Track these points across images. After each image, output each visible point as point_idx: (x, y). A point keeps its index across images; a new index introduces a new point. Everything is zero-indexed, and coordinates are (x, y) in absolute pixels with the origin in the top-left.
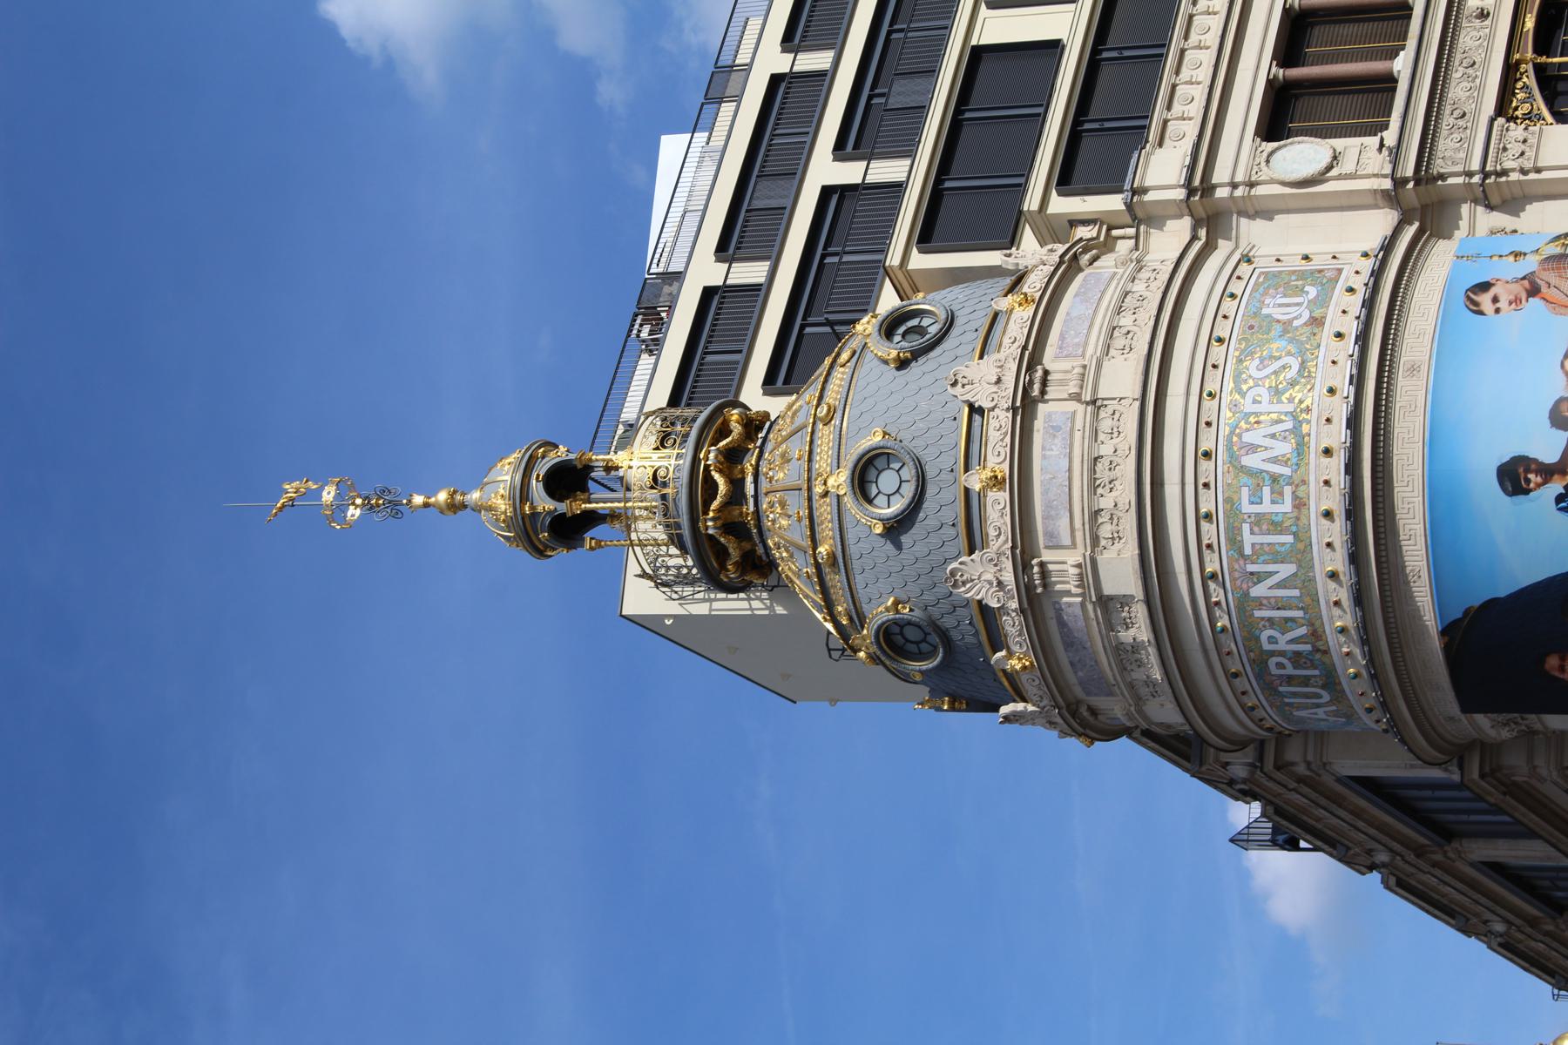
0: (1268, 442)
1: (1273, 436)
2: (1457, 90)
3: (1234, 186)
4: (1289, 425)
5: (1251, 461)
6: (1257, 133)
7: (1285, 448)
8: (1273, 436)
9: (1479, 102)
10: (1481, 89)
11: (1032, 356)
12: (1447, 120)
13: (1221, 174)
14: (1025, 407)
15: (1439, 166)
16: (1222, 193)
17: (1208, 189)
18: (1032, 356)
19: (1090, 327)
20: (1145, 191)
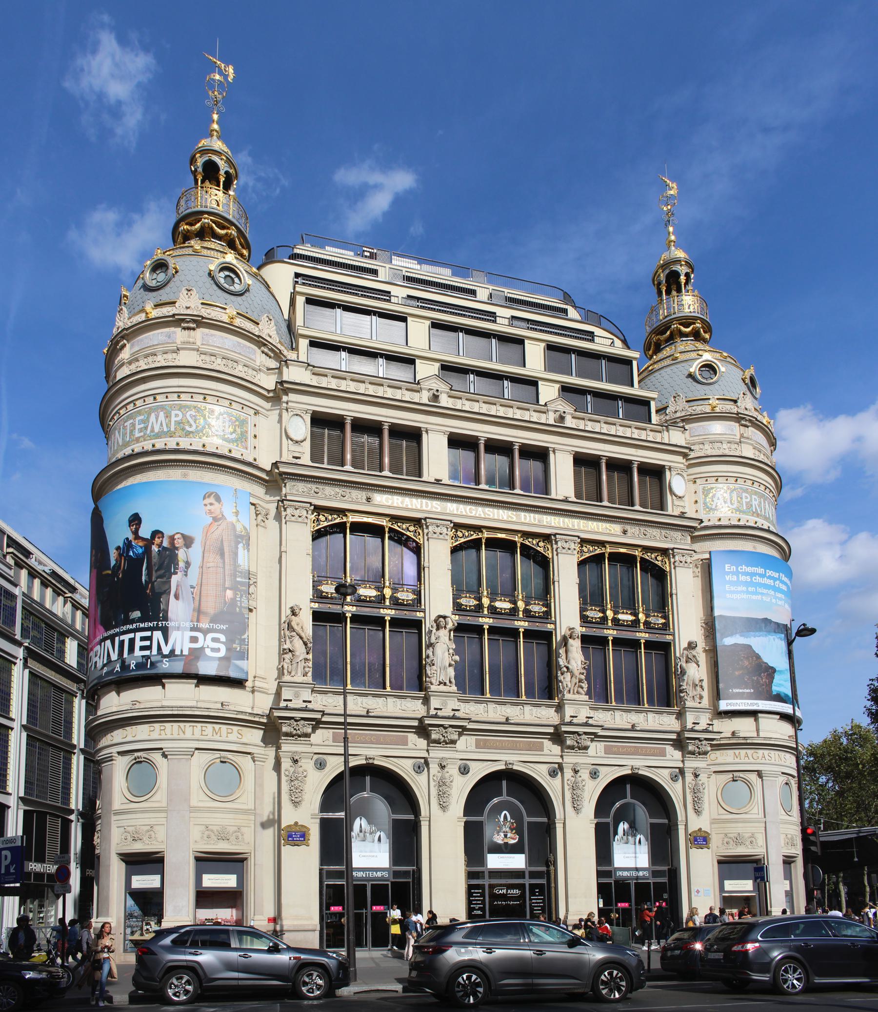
0: (159, 422)
1: (161, 424)
2: (329, 490)
3: (287, 403)
4: (165, 430)
5: (153, 416)
6: (314, 412)
7: (157, 430)
8: (161, 424)
9: (322, 499)
10: (330, 499)
11: (200, 322)
12: (313, 487)
13: (292, 397)
14: (177, 321)
15: (290, 484)
16: (285, 398)
17: (286, 391)
18: (200, 322)
19: (218, 347)
20: (288, 367)
